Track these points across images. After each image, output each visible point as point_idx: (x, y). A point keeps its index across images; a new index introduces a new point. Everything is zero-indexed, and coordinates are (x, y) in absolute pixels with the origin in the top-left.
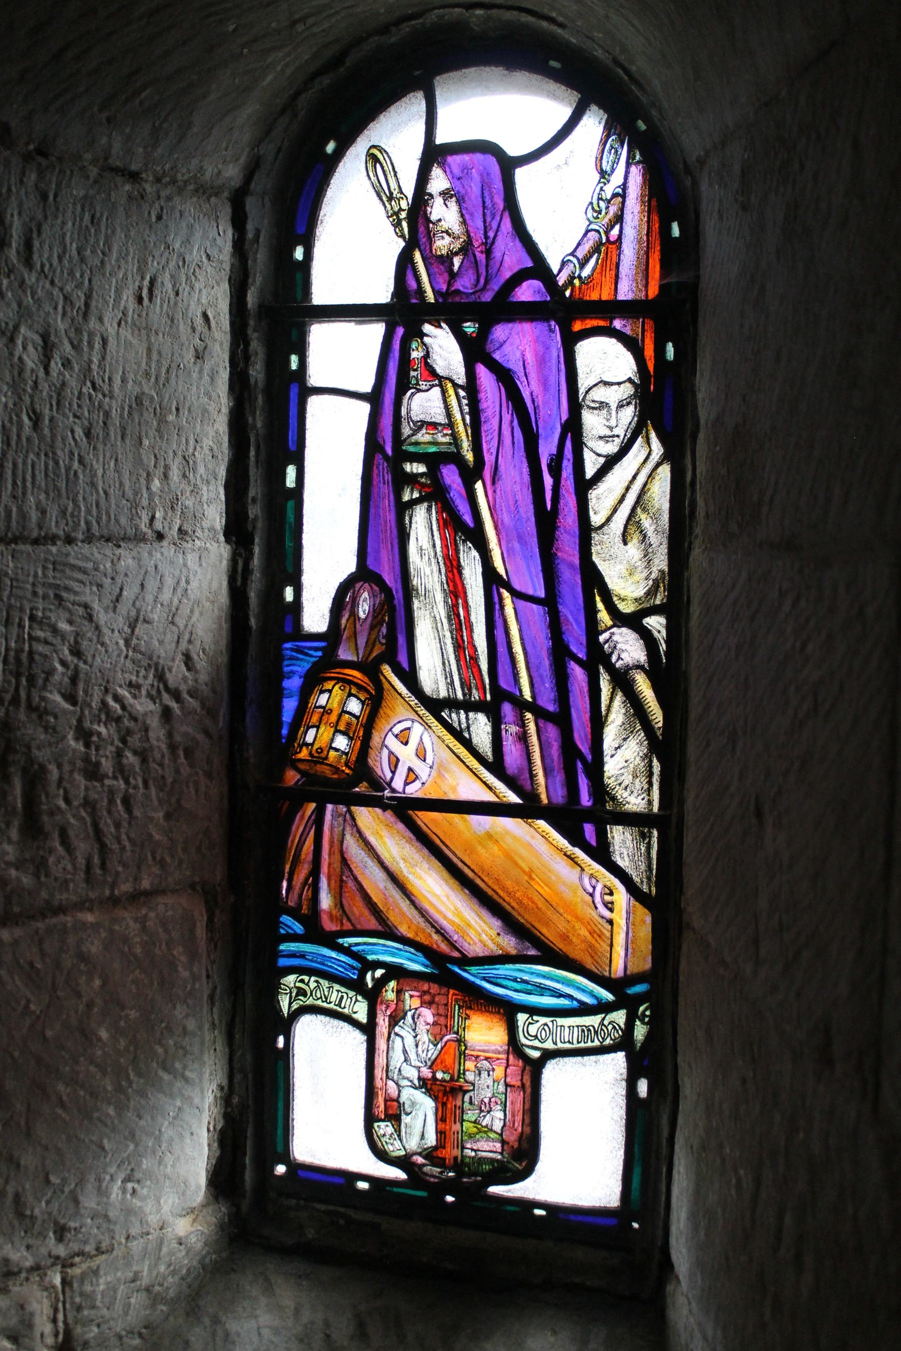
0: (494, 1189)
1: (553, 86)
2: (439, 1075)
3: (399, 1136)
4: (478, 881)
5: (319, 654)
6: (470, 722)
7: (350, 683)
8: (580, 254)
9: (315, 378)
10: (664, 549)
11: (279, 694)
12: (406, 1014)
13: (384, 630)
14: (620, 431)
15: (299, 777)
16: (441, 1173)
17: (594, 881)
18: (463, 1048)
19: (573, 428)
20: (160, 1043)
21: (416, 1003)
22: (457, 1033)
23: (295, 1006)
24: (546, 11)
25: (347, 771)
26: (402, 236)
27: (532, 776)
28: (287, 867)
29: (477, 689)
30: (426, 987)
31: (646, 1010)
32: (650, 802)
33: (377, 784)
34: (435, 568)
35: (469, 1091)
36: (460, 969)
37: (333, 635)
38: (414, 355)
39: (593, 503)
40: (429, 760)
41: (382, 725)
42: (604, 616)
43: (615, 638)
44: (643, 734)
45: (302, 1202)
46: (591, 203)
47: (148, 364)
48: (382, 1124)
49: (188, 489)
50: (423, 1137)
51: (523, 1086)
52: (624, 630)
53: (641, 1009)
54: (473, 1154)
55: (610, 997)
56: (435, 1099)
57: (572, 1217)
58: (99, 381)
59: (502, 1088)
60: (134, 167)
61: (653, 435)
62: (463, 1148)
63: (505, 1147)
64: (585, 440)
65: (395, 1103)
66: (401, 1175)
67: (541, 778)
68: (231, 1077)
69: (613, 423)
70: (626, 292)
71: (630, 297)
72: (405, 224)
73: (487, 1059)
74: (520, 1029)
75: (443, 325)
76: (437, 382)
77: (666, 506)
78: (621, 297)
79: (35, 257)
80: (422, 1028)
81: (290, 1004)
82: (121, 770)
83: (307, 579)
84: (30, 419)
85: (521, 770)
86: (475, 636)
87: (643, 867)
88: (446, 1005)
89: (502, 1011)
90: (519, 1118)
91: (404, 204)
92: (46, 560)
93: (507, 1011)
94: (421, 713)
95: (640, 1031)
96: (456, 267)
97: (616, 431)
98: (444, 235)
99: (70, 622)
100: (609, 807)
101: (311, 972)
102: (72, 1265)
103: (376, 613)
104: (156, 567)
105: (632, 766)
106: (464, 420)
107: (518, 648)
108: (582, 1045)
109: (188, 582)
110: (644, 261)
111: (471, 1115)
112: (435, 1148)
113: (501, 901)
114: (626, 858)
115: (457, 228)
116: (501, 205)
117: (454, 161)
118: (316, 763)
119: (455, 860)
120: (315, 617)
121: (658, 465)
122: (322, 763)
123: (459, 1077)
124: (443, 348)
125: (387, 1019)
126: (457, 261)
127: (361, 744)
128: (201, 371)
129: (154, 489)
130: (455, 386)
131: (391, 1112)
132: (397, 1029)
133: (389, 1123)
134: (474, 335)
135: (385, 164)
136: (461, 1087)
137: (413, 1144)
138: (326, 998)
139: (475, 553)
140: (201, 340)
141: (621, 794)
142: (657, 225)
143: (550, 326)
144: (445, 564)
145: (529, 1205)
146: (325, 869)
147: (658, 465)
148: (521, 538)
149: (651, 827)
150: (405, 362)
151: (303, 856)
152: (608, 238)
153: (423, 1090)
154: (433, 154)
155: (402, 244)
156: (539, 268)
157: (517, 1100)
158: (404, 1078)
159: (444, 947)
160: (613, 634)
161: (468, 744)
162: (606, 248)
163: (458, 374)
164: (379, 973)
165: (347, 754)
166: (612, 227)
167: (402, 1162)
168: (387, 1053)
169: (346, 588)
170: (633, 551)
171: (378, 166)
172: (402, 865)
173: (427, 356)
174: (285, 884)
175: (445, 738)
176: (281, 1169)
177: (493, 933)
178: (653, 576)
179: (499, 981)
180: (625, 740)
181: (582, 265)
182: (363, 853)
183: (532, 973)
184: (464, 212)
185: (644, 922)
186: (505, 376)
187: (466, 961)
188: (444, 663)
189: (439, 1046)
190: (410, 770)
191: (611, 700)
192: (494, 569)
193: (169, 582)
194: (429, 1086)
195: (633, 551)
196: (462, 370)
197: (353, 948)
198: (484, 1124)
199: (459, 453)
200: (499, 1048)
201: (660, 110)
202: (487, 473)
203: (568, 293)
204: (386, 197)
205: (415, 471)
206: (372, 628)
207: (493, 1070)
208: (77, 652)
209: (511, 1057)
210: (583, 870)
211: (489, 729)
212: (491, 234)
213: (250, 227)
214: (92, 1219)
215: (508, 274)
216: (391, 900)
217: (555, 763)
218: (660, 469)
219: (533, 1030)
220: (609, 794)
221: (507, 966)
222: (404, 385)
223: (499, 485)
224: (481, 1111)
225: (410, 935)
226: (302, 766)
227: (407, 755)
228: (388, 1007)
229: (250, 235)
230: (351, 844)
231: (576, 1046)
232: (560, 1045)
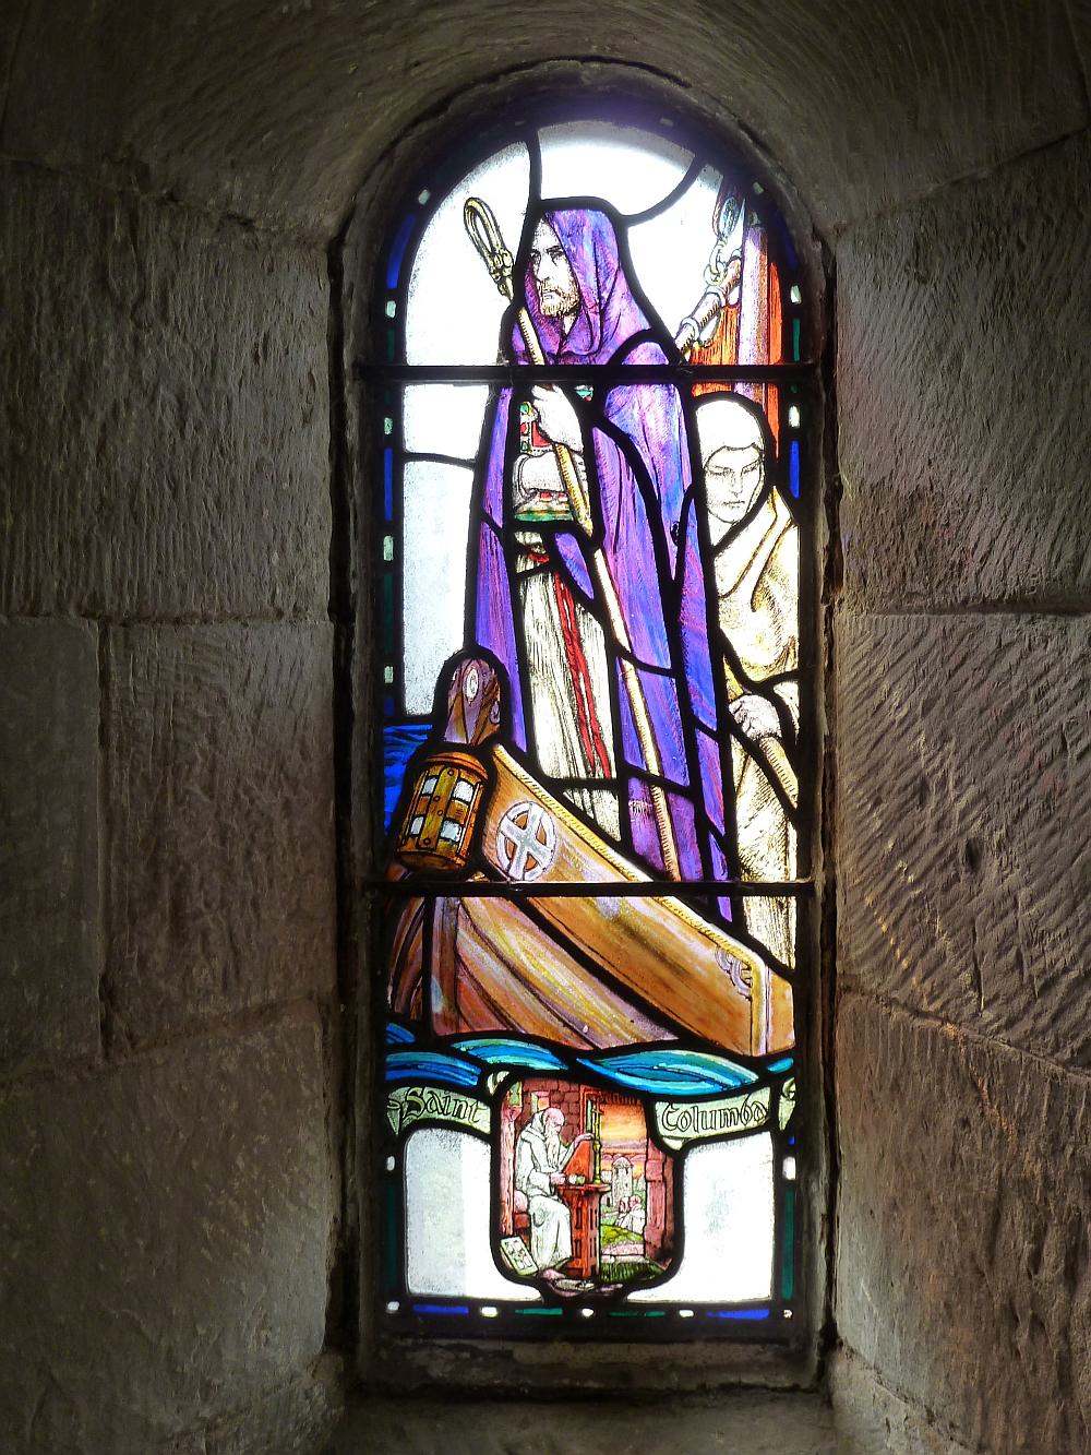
0: (636, 1296)
1: (664, 143)
2: (573, 1179)
3: (529, 1251)
5: (425, 737)
6: (595, 801)
8: (701, 315)
9: (413, 443)
12: (533, 1117)
13: (496, 709)
14: (745, 496)
15: (404, 870)
16: (578, 1285)
17: (730, 958)
18: (598, 1146)
19: (697, 494)
20: (286, 1171)
22: (591, 1132)
23: (407, 1122)
24: (670, 69)
26: (507, 294)
27: (662, 853)
29: (602, 765)
30: (554, 1085)
31: (791, 1084)
33: (491, 871)
35: (606, 1192)
36: (592, 1062)
38: (524, 419)
40: (550, 845)
41: (497, 809)
43: (745, 707)
44: (778, 802)
45: (421, 1341)
46: (709, 265)
47: (265, 428)
49: (302, 563)
51: (664, 1179)
53: (786, 1084)
54: (613, 1260)
55: (753, 1077)
56: (569, 1204)
57: (722, 1315)
58: (226, 446)
59: (642, 1185)
60: (251, 214)
61: (779, 500)
62: (601, 1254)
63: (647, 1248)
64: (710, 506)
65: (524, 1215)
66: (532, 1294)
67: (672, 855)
69: (737, 489)
70: (748, 356)
71: (752, 362)
72: (509, 282)
73: (624, 1155)
74: (659, 1121)
75: (554, 387)
76: (551, 447)
78: (743, 362)
79: (171, 312)
80: (552, 1131)
81: (401, 1119)
83: (409, 657)
84: (170, 487)
85: (651, 848)
87: (782, 939)
88: (577, 1102)
89: (638, 1102)
91: (508, 261)
92: (186, 640)
94: (539, 795)
95: (786, 1109)
96: (567, 330)
97: (740, 498)
98: (553, 294)
99: (207, 708)
100: (745, 878)
101: (423, 1083)
102: (216, 1427)
103: (486, 693)
104: (277, 648)
105: (767, 836)
106: (581, 487)
108: (726, 1130)
109: (302, 664)
111: (608, 1219)
112: (571, 1259)
114: (764, 929)
115: (567, 288)
117: (564, 216)
118: (424, 855)
119: (582, 948)
120: (419, 698)
121: (785, 530)
122: (431, 855)
123: (594, 1178)
124: (555, 411)
125: (512, 1125)
126: (568, 322)
127: (473, 832)
128: (309, 434)
129: (274, 563)
130: (571, 451)
131: (520, 1226)
132: (524, 1134)
133: (518, 1239)
134: (590, 399)
135: (485, 218)
136: (597, 1189)
137: (545, 1258)
138: (443, 1110)
139: (596, 624)
140: (307, 401)
141: (755, 865)
143: (669, 390)
144: (564, 637)
145: (672, 1308)
146: (435, 968)
147: (785, 530)
148: (645, 609)
149: (788, 896)
150: (515, 427)
151: (410, 957)
153: (556, 1197)
154: (539, 210)
155: (508, 303)
156: (655, 331)
157: (659, 1196)
158: (534, 1187)
159: (574, 1042)
162: (727, 312)
164: (501, 1076)
167: (537, 1280)
168: (514, 1162)
169: (452, 666)
171: (478, 219)
172: (523, 957)
175: (567, 819)
176: (393, 1306)
179: (634, 1071)
181: (701, 329)
182: (479, 948)
184: (576, 270)
185: (784, 996)
186: (624, 441)
187: (598, 1054)
188: (564, 741)
189: (571, 1148)
190: (529, 854)
192: (617, 640)
193: (287, 664)
194: (562, 1192)
197: (471, 1052)
198: (623, 1226)
199: (576, 520)
200: (637, 1143)
201: (789, 176)
202: (608, 541)
203: (687, 356)
204: (490, 253)
205: (528, 541)
206: (482, 708)
207: (632, 1166)
208: (213, 739)
209: (650, 1150)
210: (719, 946)
212: (605, 295)
213: (346, 280)
214: (233, 1374)
220: (743, 866)
222: (514, 449)
223: (621, 553)
224: (620, 1212)
229: (345, 290)
230: (464, 936)
231: (719, 1131)
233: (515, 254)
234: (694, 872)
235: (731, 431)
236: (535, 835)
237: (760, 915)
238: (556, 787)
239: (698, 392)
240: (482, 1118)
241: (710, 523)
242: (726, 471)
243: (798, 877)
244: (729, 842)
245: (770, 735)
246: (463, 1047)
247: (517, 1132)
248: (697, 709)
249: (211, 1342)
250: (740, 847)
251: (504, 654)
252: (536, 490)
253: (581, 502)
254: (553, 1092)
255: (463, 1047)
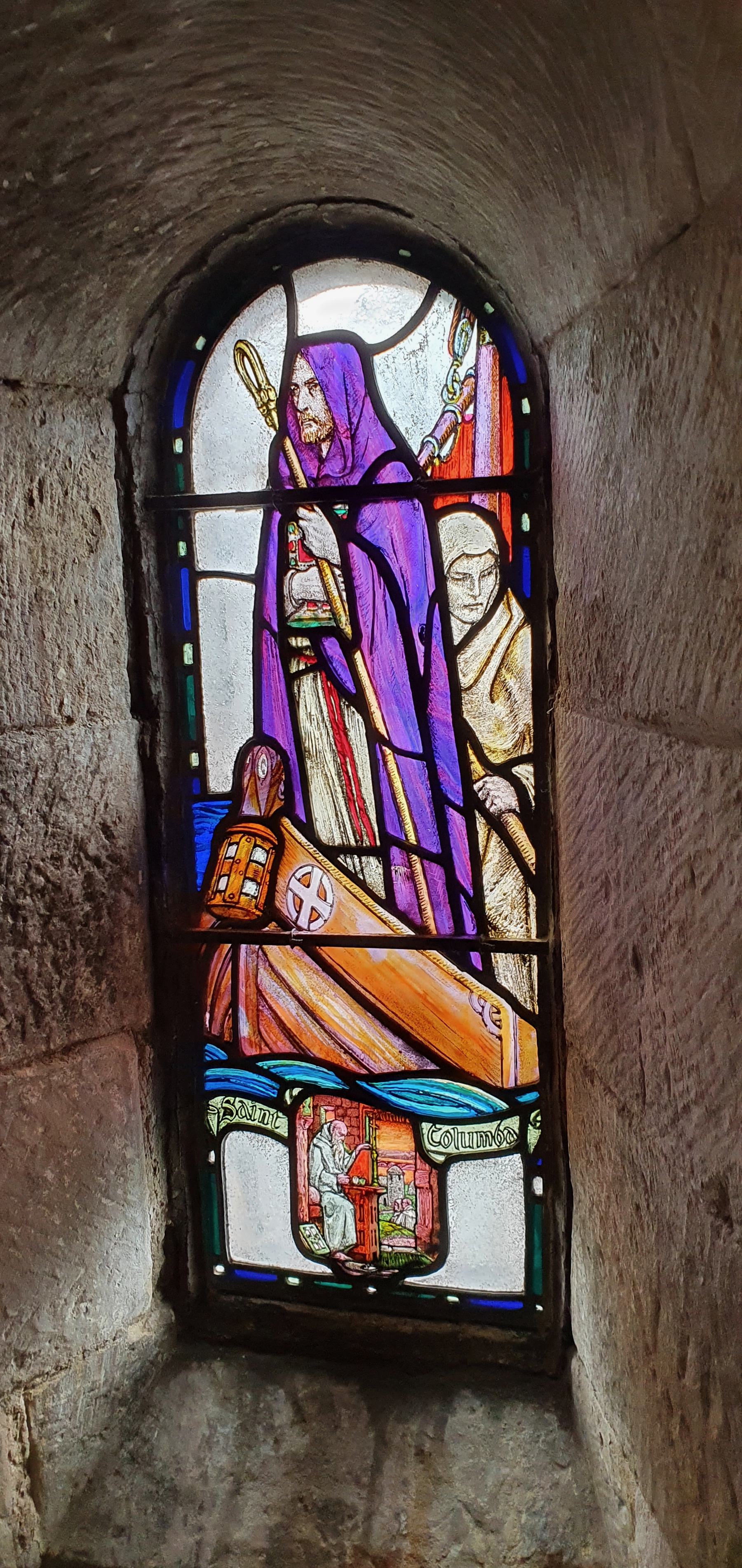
2: (355, 1181)
4: (379, 1005)
5: (226, 811)
7: (255, 835)
10: (528, 705)
11: (191, 849)
12: (322, 1127)
13: (282, 788)
14: (483, 599)
15: (214, 920)
16: (362, 1267)
17: (482, 1001)
19: (440, 599)
20: (102, 1175)
21: (331, 1116)
22: (369, 1142)
23: (223, 1125)
25: (258, 913)
26: (273, 426)
27: (421, 911)
28: (209, 1000)
30: (338, 1101)
31: (537, 1116)
32: (528, 930)
33: (285, 923)
34: (324, 731)
37: (237, 794)
38: (292, 537)
39: (461, 666)
42: (477, 767)
43: (488, 786)
46: (446, 385)
48: (308, 1226)
49: (93, 674)
50: (344, 1236)
51: (431, 1187)
52: (496, 778)
53: (533, 1115)
55: (504, 1106)
56: (353, 1202)
59: (412, 1190)
61: (513, 601)
62: (381, 1244)
64: (451, 609)
67: (429, 912)
68: (169, 1194)
71: (486, 474)
72: (274, 414)
73: (397, 1164)
74: (425, 1137)
77: (529, 665)
78: (478, 474)
81: (219, 1122)
82: (47, 935)
85: (410, 905)
86: (363, 790)
87: (526, 988)
90: (429, 1216)
93: (414, 1121)
95: (533, 1136)
96: (324, 454)
97: (479, 600)
100: (492, 935)
103: (273, 772)
106: (340, 596)
107: (401, 799)
108: (482, 1148)
110: (498, 438)
111: (386, 1215)
112: (356, 1245)
113: (400, 1022)
114: (510, 980)
115: (323, 416)
116: (362, 392)
119: (358, 987)
120: (220, 780)
122: (234, 907)
126: (325, 447)
130: (331, 565)
132: (315, 1141)
136: (375, 1190)
137: (336, 1243)
139: (358, 716)
142: (509, 403)
145: (441, 1293)
150: (284, 546)
151: (222, 990)
152: (463, 418)
154: (297, 346)
155: (274, 433)
156: (401, 452)
157: (427, 1200)
158: (324, 1184)
159: (352, 1066)
160: (486, 782)
161: (363, 885)
162: (463, 428)
163: (333, 554)
164: (296, 1091)
165: (256, 898)
166: (467, 408)
170: (500, 707)
171: (246, 359)
172: (311, 993)
173: (304, 538)
174: (208, 1015)
176: (220, 1269)
177: (396, 1051)
178: (519, 729)
179: (403, 1094)
180: (502, 875)
181: (441, 446)
183: (432, 1086)
185: (530, 1037)
186: (375, 553)
187: (373, 1077)
188: (337, 815)
190: (313, 909)
191: (488, 840)
192: (377, 730)
195: (500, 707)
196: (336, 550)
199: (338, 626)
202: (365, 643)
203: (429, 472)
206: (271, 785)
207: (403, 1174)
209: (418, 1161)
210: (472, 992)
211: (380, 870)
212: (355, 420)
213: (130, 424)
215: (373, 458)
216: (303, 1025)
217: (441, 899)
218: (521, 632)
219: (437, 1137)
220: (490, 924)
221: (409, 1080)
222: (284, 567)
224: (395, 1211)
225: (321, 1056)
226: (217, 911)
227: (310, 897)
228: (306, 1121)
232: (462, 1150)
233: (278, 389)
234: (447, 928)
235: (469, 540)
236: (317, 895)
237: (506, 966)
238: (331, 853)
239: (439, 504)
240: (282, 1126)
241: (453, 624)
242: (466, 576)
243: (537, 937)
244: (477, 902)
245: (510, 811)
246: (264, 1064)
247: (310, 1139)
248: (445, 787)
249: (24, 1320)
250: (487, 906)
251: (285, 741)
252: (304, 600)
253: (342, 613)
254: (338, 1107)
255: (264, 1064)
